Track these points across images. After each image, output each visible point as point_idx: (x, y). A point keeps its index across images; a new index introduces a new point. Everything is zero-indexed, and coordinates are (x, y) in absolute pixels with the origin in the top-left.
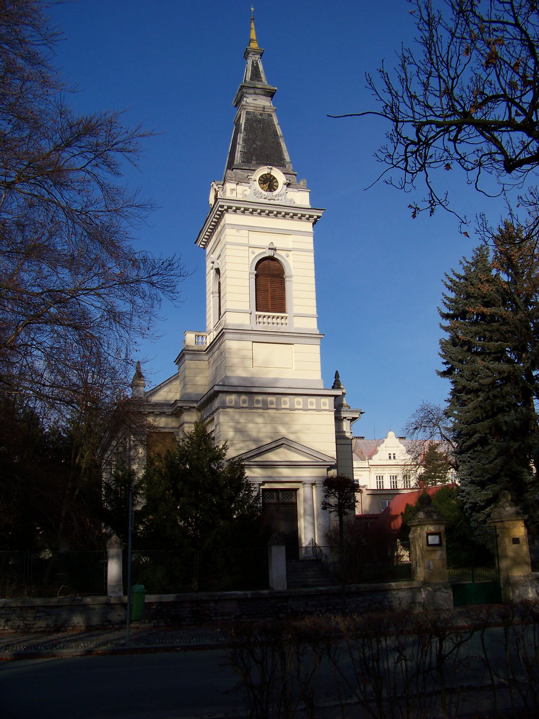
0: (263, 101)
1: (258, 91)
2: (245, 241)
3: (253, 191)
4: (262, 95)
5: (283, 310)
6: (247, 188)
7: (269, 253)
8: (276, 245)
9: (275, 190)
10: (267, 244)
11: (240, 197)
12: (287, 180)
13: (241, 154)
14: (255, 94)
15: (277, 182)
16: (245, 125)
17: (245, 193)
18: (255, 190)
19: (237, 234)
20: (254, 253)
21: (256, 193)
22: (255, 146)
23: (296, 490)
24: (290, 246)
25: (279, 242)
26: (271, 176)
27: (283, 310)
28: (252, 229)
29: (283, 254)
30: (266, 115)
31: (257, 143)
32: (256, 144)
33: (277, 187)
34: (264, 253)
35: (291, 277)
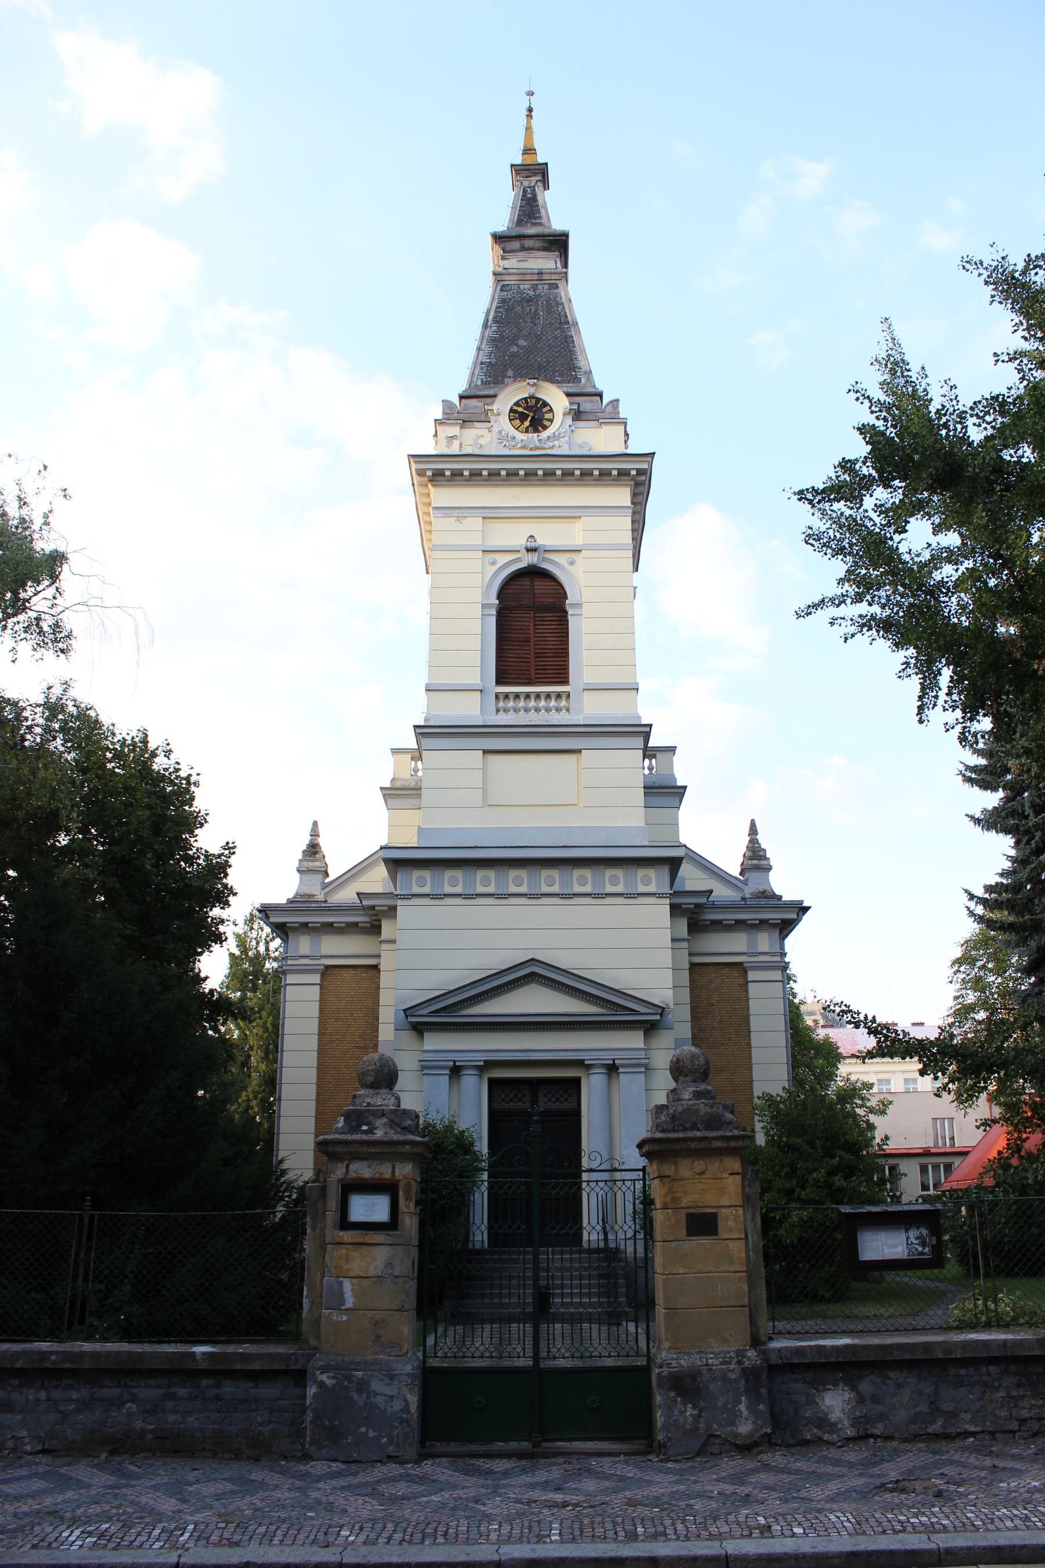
0: (540, 261)
1: (528, 243)
2: (476, 539)
3: (495, 435)
4: (538, 249)
5: (565, 681)
6: (485, 432)
7: (527, 560)
8: (541, 541)
9: (545, 428)
10: (521, 542)
11: (468, 450)
12: (571, 404)
13: (482, 369)
14: (523, 249)
15: (551, 410)
16: (496, 312)
17: (481, 441)
18: (500, 432)
19: (458, 526)
20: (494, 563)
21: (502, 438)
22: (515, 349)
23: (576, 1082)
24: (578, 541)
25: (548, 535)
26: (538, 400)
27: (565, 681)
28: (490, 515)
29: (561, 559)
30: (546, 287)
31: (522, 342)
32: (517, 345)
33: (551, 421)
34: (519, 560)
35: (579, 605)
